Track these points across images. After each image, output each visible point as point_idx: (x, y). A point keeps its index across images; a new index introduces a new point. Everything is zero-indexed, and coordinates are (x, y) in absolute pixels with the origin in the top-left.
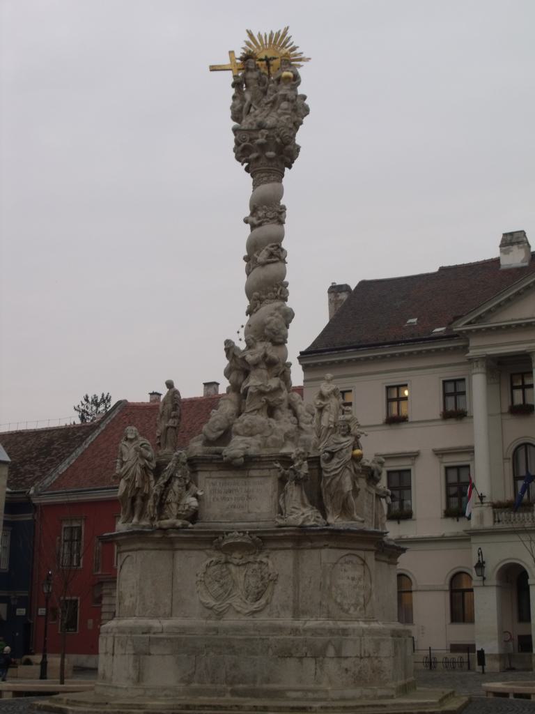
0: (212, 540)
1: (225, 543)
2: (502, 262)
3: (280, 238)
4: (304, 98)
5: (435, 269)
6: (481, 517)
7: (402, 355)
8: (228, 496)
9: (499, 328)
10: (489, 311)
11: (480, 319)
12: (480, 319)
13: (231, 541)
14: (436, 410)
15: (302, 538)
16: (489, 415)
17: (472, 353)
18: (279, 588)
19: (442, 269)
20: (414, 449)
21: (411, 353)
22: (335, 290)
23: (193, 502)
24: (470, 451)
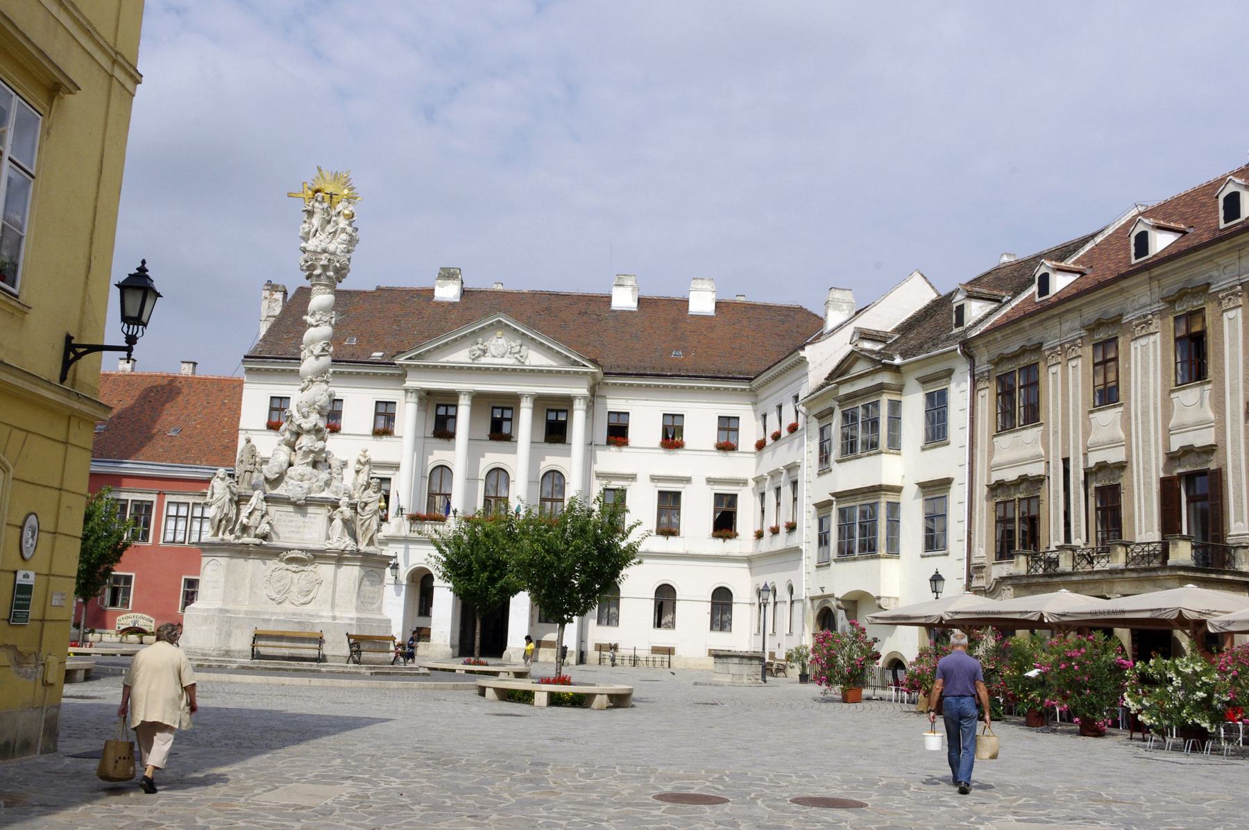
0: (276, 553)
5: (374, 289)
6: (399, 527)
9: (435, 367)
11: (419, 357)
12: (419, 357)
14: (368, 427)
15: (340, 558)
16: (416, 438)
18: (322, 588)
19: (379, 289)
21: (350, 373)
23: (267, 528)
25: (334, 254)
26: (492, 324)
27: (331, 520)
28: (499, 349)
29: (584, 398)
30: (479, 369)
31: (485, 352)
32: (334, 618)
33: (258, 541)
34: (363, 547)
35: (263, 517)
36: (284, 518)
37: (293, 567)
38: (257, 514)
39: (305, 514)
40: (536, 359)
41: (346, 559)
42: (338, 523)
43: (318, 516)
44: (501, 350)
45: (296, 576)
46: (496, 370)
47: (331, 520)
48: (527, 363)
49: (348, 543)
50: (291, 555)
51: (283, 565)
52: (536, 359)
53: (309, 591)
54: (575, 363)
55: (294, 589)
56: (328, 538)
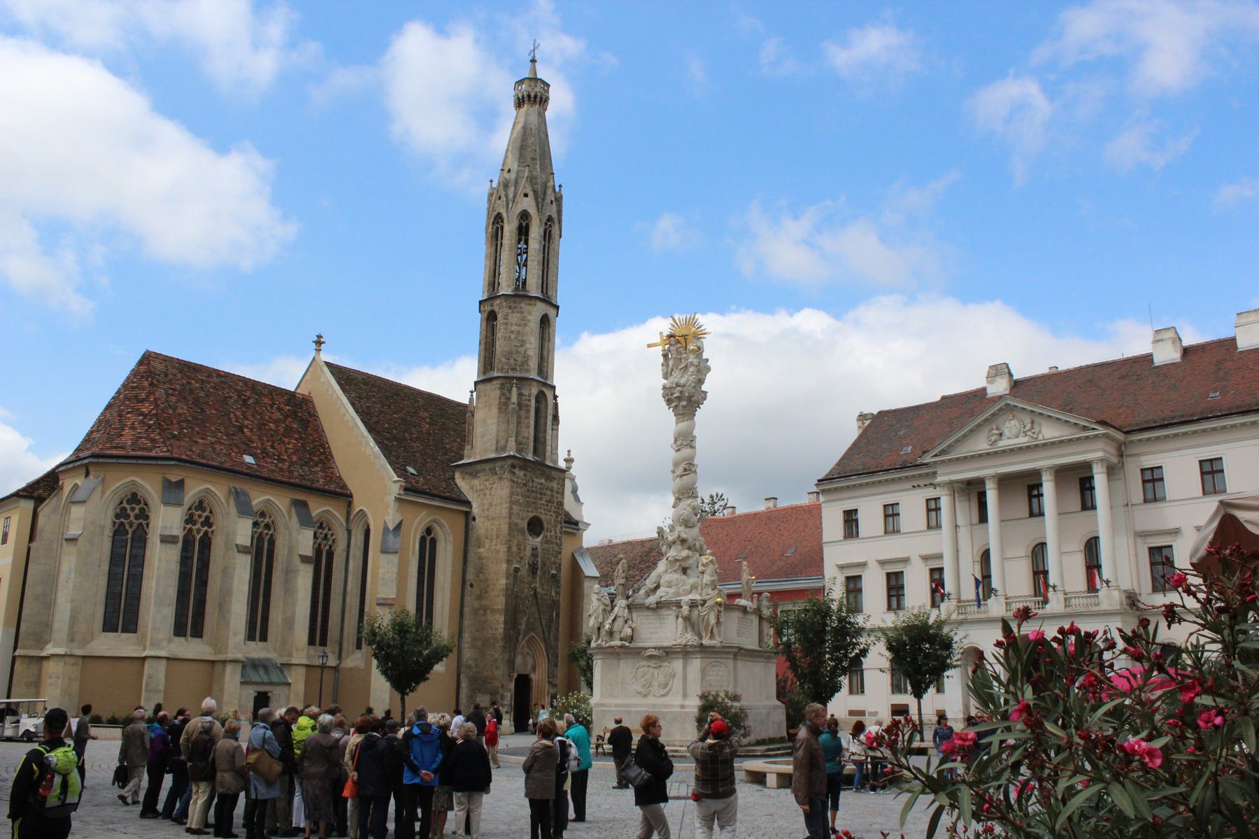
0: (637, 653)
2: (989, 391)
3: (692, 458)
4: (707, 360)
5: (938, 399)
7: (893, 480)
10: (950, 446)
12: (943, 452)
17: (939, 479)
19: (944, 398)
20: (905, 555)
21: (900, 479)
22: (862, 417)
24: (939, 557)
25: (684, 386)
26: (1001, 409)
28: (1013, 432)
29: (1102, 460)
30: (996, 453)
31: (1001, 434)
32: (683, 707)
34: (706, 642)
37: (652, 663)
40: (1049, 432)
43: (669, 616)
44: (1014, 431)
45: (656, 672)
46: (1012, 450)
48: (1040, 437)
50: (649, 653)
51: (645, 663)
52: (1049, 432)
53: (666, 685)
54: (1085, 428)
55: (655, 683)
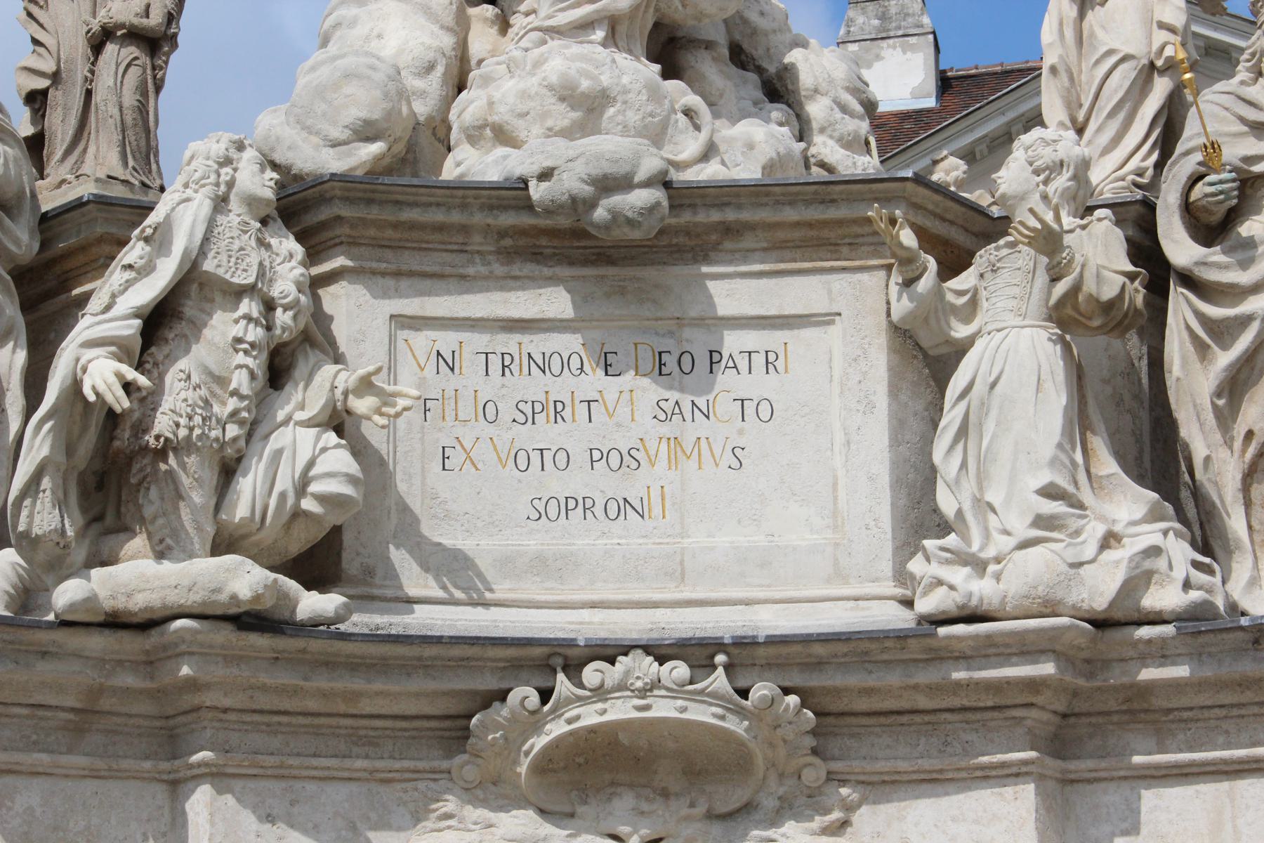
1: (556, 729)
8: (546, 433)
13: (590, 716)
27: (926, 360)
33: (244, 579)
35: (278, 370)
36: (471, 377)
38: (223, 343)
39: (683, 358)
41: (1147, 712)
42: (1014, 353)
43: (810, 348)
47: (926, 360)
49: (1119, 541)
50: (582, 712)
56: (920, 518)
